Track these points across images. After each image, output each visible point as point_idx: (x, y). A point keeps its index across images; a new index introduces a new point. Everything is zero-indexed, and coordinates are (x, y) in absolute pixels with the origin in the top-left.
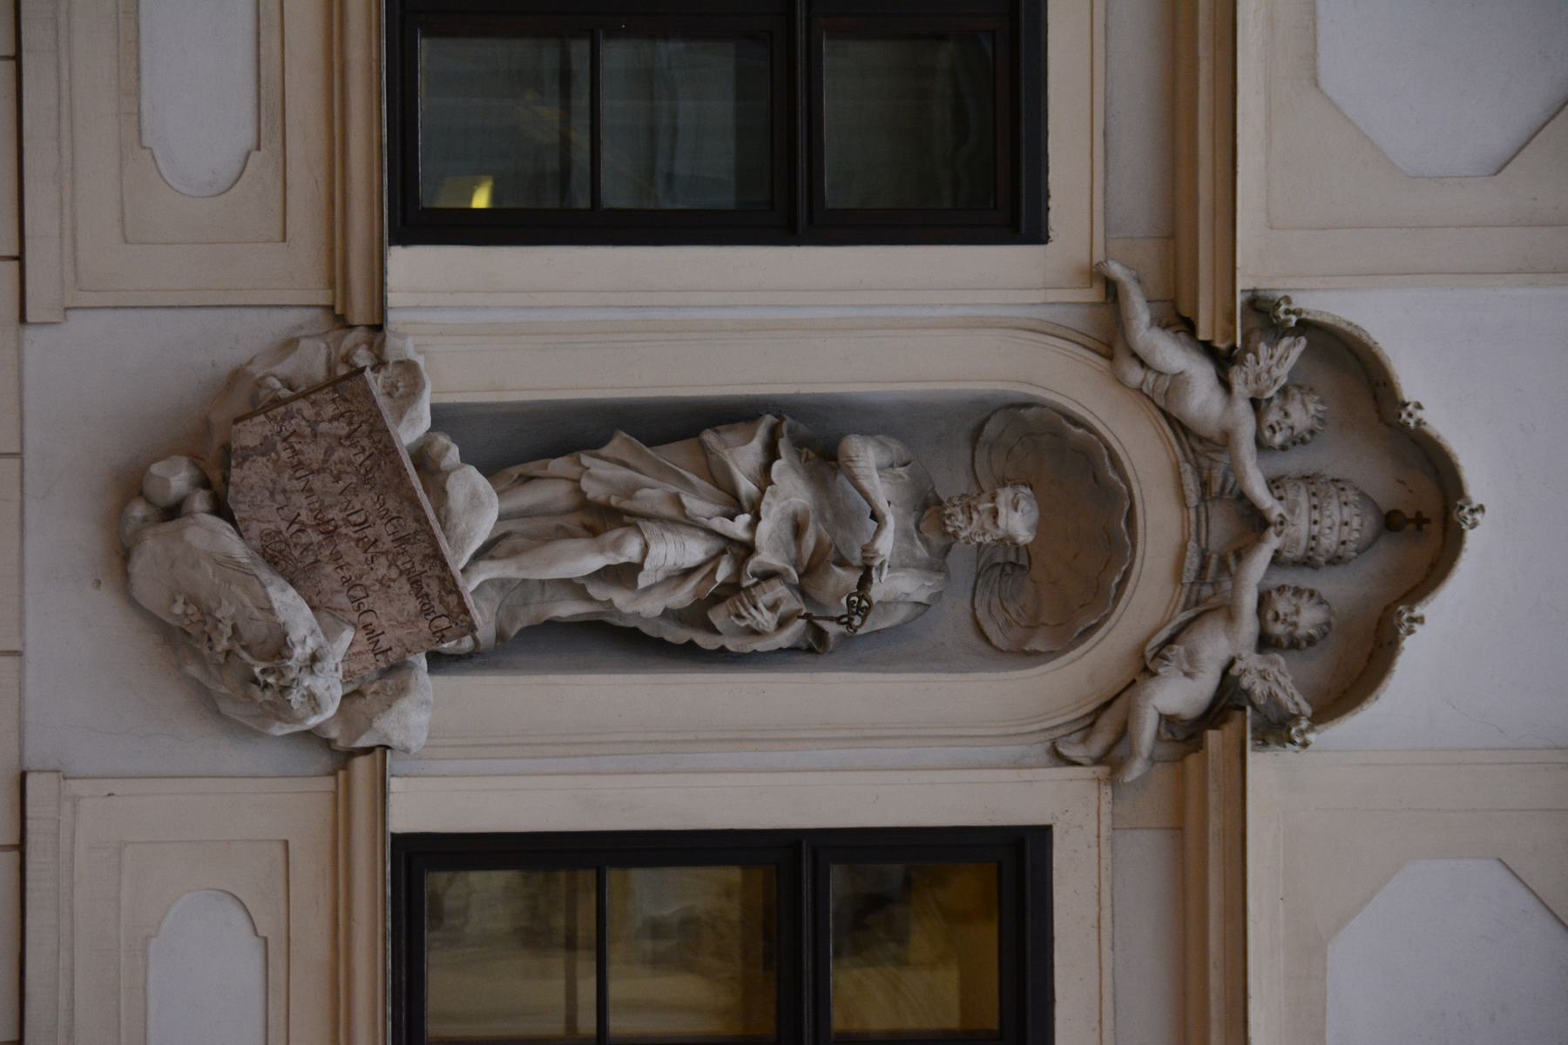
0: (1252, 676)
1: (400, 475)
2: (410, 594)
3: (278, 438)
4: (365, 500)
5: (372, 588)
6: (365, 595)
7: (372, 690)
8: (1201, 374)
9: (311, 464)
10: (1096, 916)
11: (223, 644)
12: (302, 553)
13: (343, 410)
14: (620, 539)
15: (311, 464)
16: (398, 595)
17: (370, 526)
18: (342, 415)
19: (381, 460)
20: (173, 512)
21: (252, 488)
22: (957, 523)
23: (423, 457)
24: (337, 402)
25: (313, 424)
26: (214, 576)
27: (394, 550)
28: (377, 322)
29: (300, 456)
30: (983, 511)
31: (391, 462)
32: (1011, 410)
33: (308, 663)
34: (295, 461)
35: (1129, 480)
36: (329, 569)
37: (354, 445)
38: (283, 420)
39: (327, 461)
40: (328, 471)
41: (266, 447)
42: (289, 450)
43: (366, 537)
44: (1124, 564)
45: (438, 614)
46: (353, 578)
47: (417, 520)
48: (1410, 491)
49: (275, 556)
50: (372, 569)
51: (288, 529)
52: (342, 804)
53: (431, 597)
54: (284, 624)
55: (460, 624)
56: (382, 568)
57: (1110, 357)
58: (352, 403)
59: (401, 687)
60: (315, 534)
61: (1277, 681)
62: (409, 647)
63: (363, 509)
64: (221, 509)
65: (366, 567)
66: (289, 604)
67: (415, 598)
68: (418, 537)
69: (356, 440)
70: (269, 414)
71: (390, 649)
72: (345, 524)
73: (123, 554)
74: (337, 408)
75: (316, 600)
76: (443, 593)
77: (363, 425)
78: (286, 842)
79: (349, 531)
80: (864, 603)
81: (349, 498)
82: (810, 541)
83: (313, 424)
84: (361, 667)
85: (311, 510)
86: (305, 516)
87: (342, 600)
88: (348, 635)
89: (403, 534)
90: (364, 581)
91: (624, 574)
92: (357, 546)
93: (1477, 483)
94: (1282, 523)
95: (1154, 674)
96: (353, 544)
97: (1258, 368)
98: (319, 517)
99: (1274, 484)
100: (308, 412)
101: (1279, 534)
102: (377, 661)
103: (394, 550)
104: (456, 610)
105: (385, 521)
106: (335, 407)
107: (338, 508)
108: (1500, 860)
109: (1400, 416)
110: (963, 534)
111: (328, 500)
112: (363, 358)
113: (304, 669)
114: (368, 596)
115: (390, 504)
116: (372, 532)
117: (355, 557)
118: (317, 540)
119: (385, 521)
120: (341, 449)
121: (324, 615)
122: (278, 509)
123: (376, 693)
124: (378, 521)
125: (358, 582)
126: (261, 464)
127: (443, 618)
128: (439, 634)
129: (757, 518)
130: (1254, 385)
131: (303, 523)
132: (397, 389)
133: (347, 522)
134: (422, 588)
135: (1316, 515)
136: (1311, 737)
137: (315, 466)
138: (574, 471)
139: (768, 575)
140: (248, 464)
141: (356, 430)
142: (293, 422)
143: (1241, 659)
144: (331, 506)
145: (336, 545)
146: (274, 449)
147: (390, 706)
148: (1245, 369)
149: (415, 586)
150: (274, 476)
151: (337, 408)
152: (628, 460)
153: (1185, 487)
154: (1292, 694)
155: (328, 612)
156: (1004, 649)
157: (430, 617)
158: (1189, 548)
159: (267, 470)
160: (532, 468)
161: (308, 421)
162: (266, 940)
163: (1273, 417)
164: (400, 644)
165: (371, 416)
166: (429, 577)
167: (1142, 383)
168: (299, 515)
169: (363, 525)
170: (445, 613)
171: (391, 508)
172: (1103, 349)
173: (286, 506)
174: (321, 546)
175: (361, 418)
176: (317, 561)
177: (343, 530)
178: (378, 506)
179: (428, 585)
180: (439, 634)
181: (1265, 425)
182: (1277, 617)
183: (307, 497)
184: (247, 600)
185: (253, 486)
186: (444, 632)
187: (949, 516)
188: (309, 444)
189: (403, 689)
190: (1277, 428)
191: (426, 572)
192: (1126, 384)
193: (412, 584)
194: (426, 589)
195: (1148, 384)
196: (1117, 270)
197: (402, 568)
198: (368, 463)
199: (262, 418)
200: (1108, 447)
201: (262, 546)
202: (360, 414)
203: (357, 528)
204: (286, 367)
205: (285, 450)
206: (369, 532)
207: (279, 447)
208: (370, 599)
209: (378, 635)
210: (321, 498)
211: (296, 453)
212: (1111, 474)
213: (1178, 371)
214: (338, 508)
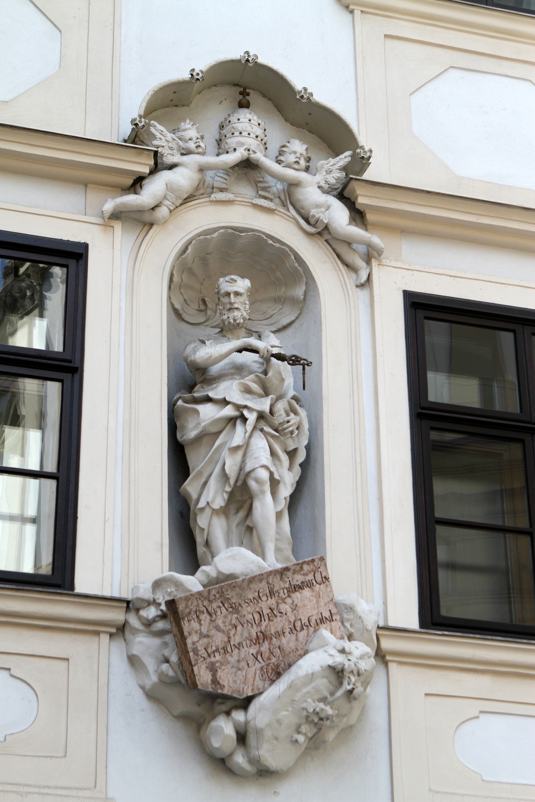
0: (329, 178)
1: (234, 587)
3: (208, 660)
4: (247, 611)
5: (297, 616)
6: (300, 621)
7: (349, 627)
8: (164, 176)
9: (225, 642)
10: (449, 277)
12: (274, 656)
13: (195, 616)
14: (257, 481)
15: (225, 642)
16: (301, 600)
17: (262, 611)
19: (226, 597)
21: (235, 682)
22: (239, 316)
24: (190, 619)
25: (203, 636)
26: (288, 711)
27: (276, 598)
28: (125, 605)
29: (220, 648)
30: (234, 300)
31: (227, 590)
32: (172, 287)
33: (344, 655)
34: (222, 651)
35: (219, 227)
36: (284, 640)
37: (215, 613)
38: (197, 655)
39: (223, 631)
40: (229, 631)
41: (213, 669)
42: (216, 654)
43: (268, 615)
44: (263, 237)
45: (313, 578)
46: (290, 626)
47: (261, 580)
48: (226, 99)
50: (286, 614)
51: (260, 663)
53: (304, 581)
55: (319, 566)
56: (285, 607)
57: (151, 225)
58: (192, 609)
59: (350, 609)
60: (264, 645)
61: (332, 166)
62: (329, 599)
63: (252, 614)
65: (284, 618)
67: (303, 590)
68: (270, 582)
69: (213, 611)
70: (193, 663)
71: (330, 611)
72: (260, 626)
74: (194, 619)
75: (301, 652)
76: (302, 573)
77: (204, 604)
78: (426, 695)
79: (264, 624)
80: (294, 358)
81: (246, 621)
82: (255, 387)
83: (203, 636)
84: (338, 630)
85: (251, 646)
86: (253, 650)
87: (302, 635)
89: (268, 591)
90: (292, 620)
91: (274, 483)
92: (272, 621)
94: (249, 150)
95: (327, 228)
96: (271, 623)
97: (166, 147)
98: (254, 642)
100: (195, 638)
101: (255, 152)
102: (336, 620)
103: (276, 598)
104: (312, 567)
105: (260, 601)
106: (193, 621)
107: (251, 629)
108: (410, 95)
109: (198, 79)
110: (245, 314)
111: (246, 634)
113: (349, 658)
114: (300, 619)
115: (251, 596)
116: (266, 610)
117: (278, 624)
119: (260, 601)
120: (217, 621)
121: (311, 646)
122: (248, 667)
123: (351, 625)
124: (260, 605)
125: (292, 624)
126: (222, 674)
127: (316, 575)
128: (324, 580)
129: (246, 407)
130: (175, 151)
131: (257, 653)
132: (173, 592)
133: (259, 625)
134: (299, 585)
135: (245, 134)
136: (367, 149)
137: (226, 639)
138: (208, 511)
140: (221, 682)
141: (207, 610)
142: (199, 648)
143: (319, 183)
144: (249, 633)
145: (271, 634)
147: (360, 618)
148: (165, 154)
149: (297, 589)
150: (229, 666)
151: (194, 619)
152: (203, 480)
153: (224, 200)
154: (341, 159)
155: (309, 643)
156: (299, 312)
158: (256, 203)
159: (226, 670)
160: (200, 540)
161: (200, 639)
162: (481, 712)
163: (192, 145)
164: (328, 604)
165: (200, 599)
166: (293, 580)
167: (169, 209)
168: (253, 654)
169: (261, 614)
170: (313, 573)
171: (254, 596)
172: (146, 228)
173: (247, 662)
174: (270, 644)
175: (201, 605)
176: (279, 648)
177: (263, 628)
178: (251, 604)
179: (297, 581)
180: (324, 580)
181: (196, 151)
182: (297, 162)
183: (243, 648)
184: (305, 690)
185: (234, 681)
186: (323, 576)
187: (235, 320)
188: (213, 640)
189: (351, 608)
190: (198, 144)
191: (290, 581)
192: (167, 218)
193: (296, 591)
194: (299, 583)
195: (170, 205)
196: (109, 206)
197: (286, 595)
198: (226, 605)
199: (195, 669)
200: (199, 235)
201: (268, 680)
202: (198, 605)
203: (263, 619)
204: (150, 664)
205: (215, 656)
206: (266, 611)
207: (213, 659)
208: (303, 618)
210: (244, 638)
211: (217, 650)
212: (215, 235)
213: (165, 186)
214: (251, 629)
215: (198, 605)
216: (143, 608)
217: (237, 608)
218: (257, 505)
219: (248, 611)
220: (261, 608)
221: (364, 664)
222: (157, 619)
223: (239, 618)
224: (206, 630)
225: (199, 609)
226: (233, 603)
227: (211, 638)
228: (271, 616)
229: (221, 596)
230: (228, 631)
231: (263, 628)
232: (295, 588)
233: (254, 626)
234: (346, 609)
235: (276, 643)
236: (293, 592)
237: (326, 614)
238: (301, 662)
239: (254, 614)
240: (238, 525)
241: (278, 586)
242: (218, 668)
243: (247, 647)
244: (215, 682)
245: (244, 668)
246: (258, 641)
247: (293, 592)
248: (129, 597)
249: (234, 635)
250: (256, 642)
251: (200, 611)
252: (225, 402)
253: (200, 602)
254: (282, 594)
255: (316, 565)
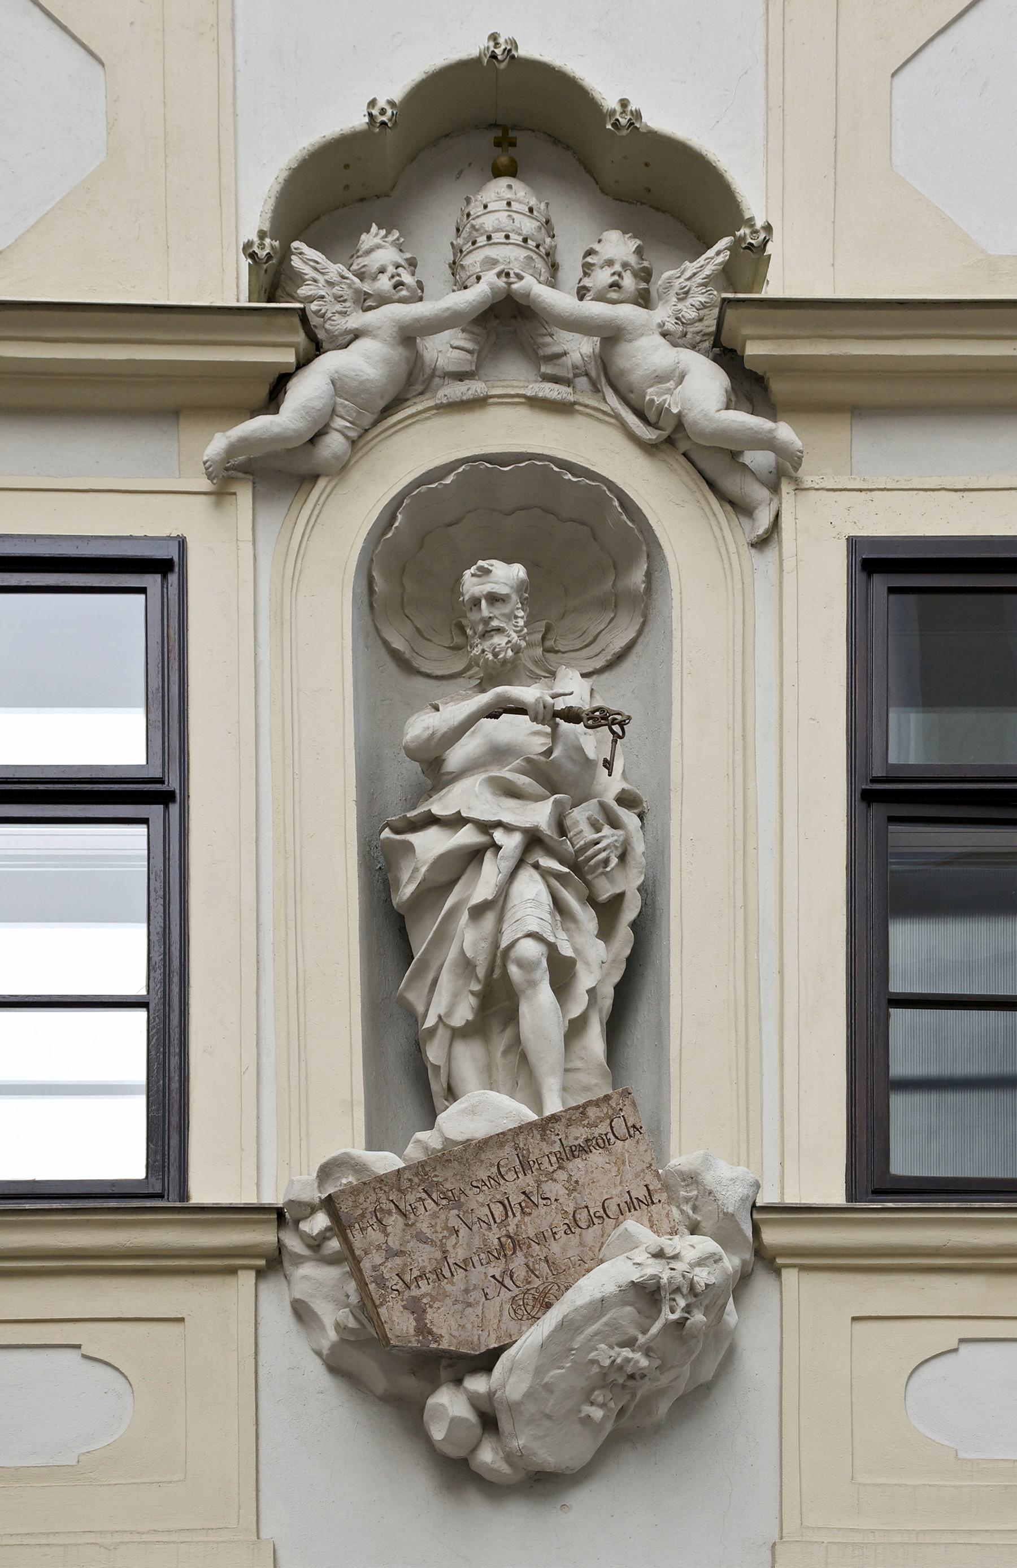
1: (449, 1161)
2: (586, 1159)
4: (477, 1201)
17: (508, 1198)
18: (380, 1221)
19: (432, 1181)
24: (365, 1226)
25: (391, 1253)
29: (427, 1271)
31: (435, 1169)
36: (555, 1247)
37: (414, 1210)
38: (384, 1287)
39: (432, 1241)
41: (416, 1308)
43: (520, 1204)
46: (567, 1221)
47: (501, 1145)
54: (619, 1287)
56: (555, 1189)
62: (645, 1166)
65: (553, 1207)
68: (521, 1145)
70: (378, 1303)
71: (646, 1186)
76: (585, 1122)
77: (391, 1198)
79: (513, 1222)
83: (391, 1253)
87: (591, 1235)
90: (570, 1210)
96: (527, 1219)
100: (377, 1258)
102: (660, 1201)
105: (502, 1182)
107: (486, 1233)
111: (477, 1242)
114: (587, 1207)
115: (483, 1175)
118: (523, 1258)
122: (487, 1299)
127: (613, 1124)
133: (504, 1223)
137: (438, 1255)
144: (485, 1240)
145: (528, 1238)
146: (416, 1300)
149: (576, 1153)
150: (449, 1301)
152: (431, 977)
157: (613, 1139)
161: (387, 1259)
168: (493, 1277)
170: (608, 1121)
173: (483, 1289)
179: (576, 1139)
186: (629, 1124)
191: (560, 1139)
193: (574, 1157)
198: (434, 1196)
199: (382, 1311)
202: (378, 1200)
203: (510, 1213)
206: (515, 1199)
207: (415, 1292)
209: (631, 1198)
211: (423, 1276)
214: (486, 1233)
215: (378, 1200)
216: (305, 1218)
217: (456, 1199)
218: (525, 1009)
219: (477, 1201)
220: (505, 1193)
221: (704, 1274)
222: (328, 1234)
223: (461, 1216)
224: (397, 1243)
225: (381, 1208)
226: (448, 1190)
227: (410, 1255)
228: (527, 1207)
229: (423, 1181)
230: (441, 1241)
231: (512, 1229)
232: (572, 1151)
233: (494, 1226)
234: (684, 1180)
235: (540, 1253)
236: (568, 1159)
237: (640, 1193)
238: (583, 1282)
239: (492, 1206)
240: (505, 1053)
241: (537, 1151)
242: (427, 1306)
243: (482, 1265)
244: (423, 1329)
245: (478, 1303)
246: (502, 1253)
247: (568, 1159)
248: (279, 1201)
249: (454, 1247)
250: (499, 1254)
251: (382, 1210)
253: (381, 1194)
254: (546, 1164)
255: (614, 1105)
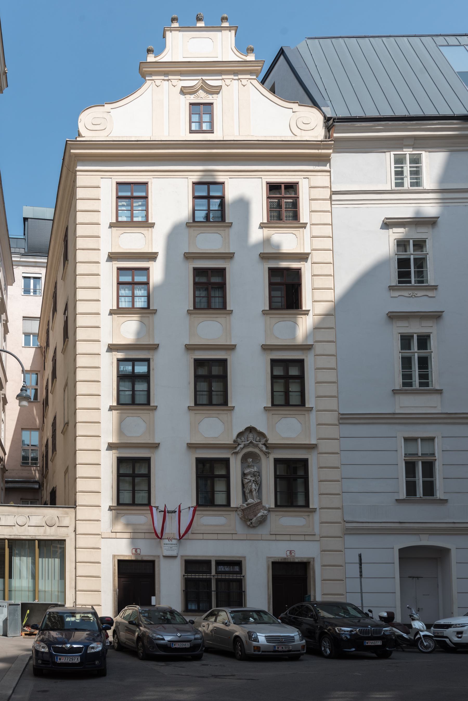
11: (262, 520)
20: (251, 523)
23: (247, 505)
41: (248, 516)
49: (255, 516)
52: (272, 511)
56: (256, 508)
57: (238, 453)
64: (252, 520)
66: (259, 515)
73: (254, 527)
82: (252, 476)
88: (261, 510)
91: (255, 489)
93: (249, 426)
99: (248, 441)
112: (240, 509)
139: (255, 479)
160: (246, 496)
163: (243, 441)
196: (232, 452)
218: (253, 493)
252: (248, 479)
